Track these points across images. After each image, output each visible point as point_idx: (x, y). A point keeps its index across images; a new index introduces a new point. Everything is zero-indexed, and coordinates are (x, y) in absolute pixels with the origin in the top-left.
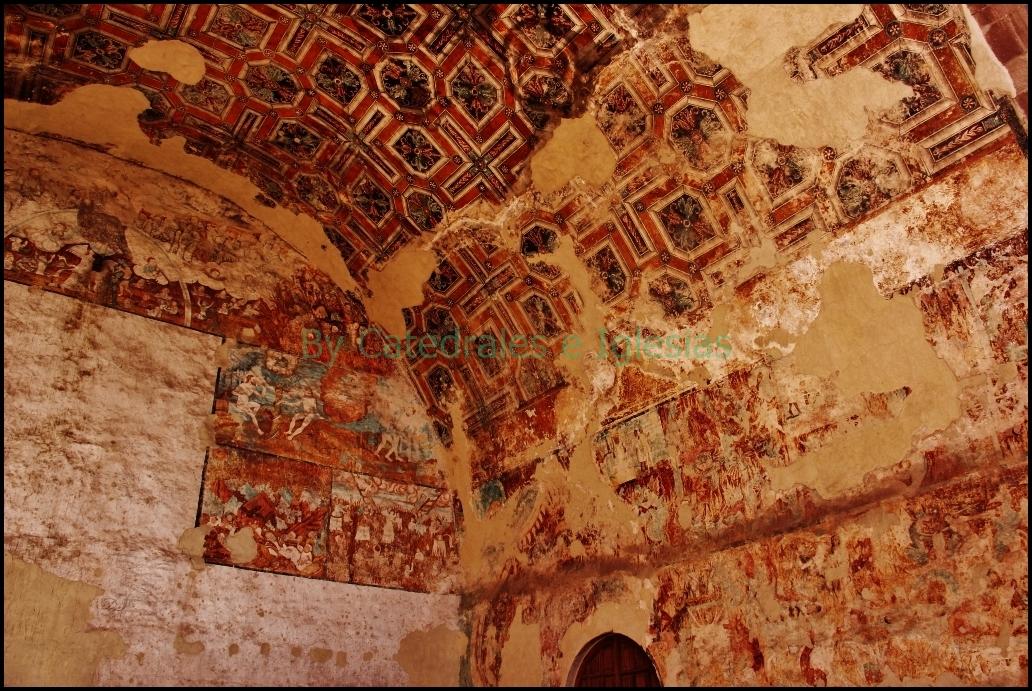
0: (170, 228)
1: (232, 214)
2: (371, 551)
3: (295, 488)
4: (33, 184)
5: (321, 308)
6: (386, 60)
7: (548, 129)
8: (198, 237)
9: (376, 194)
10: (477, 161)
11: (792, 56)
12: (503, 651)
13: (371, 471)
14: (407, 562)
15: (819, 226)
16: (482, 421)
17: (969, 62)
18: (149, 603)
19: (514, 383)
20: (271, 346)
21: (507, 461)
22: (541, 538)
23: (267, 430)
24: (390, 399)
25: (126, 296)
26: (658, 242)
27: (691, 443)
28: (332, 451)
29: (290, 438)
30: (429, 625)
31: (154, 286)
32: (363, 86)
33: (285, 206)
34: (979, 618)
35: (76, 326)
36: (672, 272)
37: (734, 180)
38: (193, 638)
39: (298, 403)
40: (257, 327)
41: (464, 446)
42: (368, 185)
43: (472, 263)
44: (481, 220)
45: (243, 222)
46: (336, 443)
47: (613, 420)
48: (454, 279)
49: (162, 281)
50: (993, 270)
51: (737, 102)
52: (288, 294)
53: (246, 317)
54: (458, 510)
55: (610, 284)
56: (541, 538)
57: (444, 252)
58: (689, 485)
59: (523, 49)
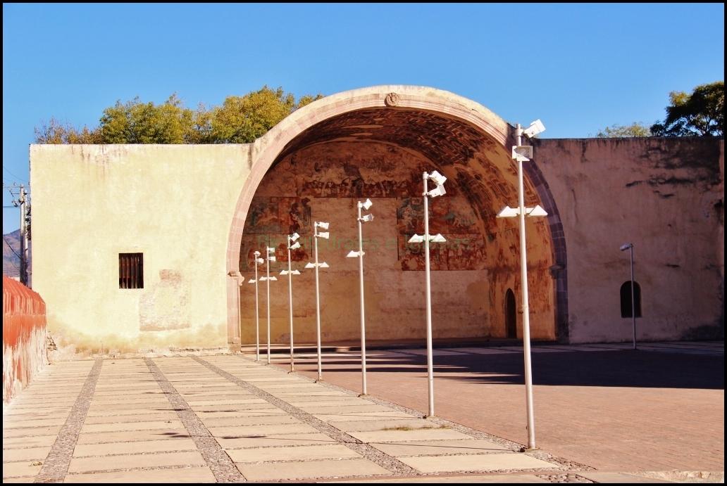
1: (391, 150)
4: (329, 162)
14: (467, 261)
25: (364, 192)
31: (371, 186)
38: (402, 292)
41: (482, 221)
46: (439, 225)
49: (374, 183)
54: (485, 241)
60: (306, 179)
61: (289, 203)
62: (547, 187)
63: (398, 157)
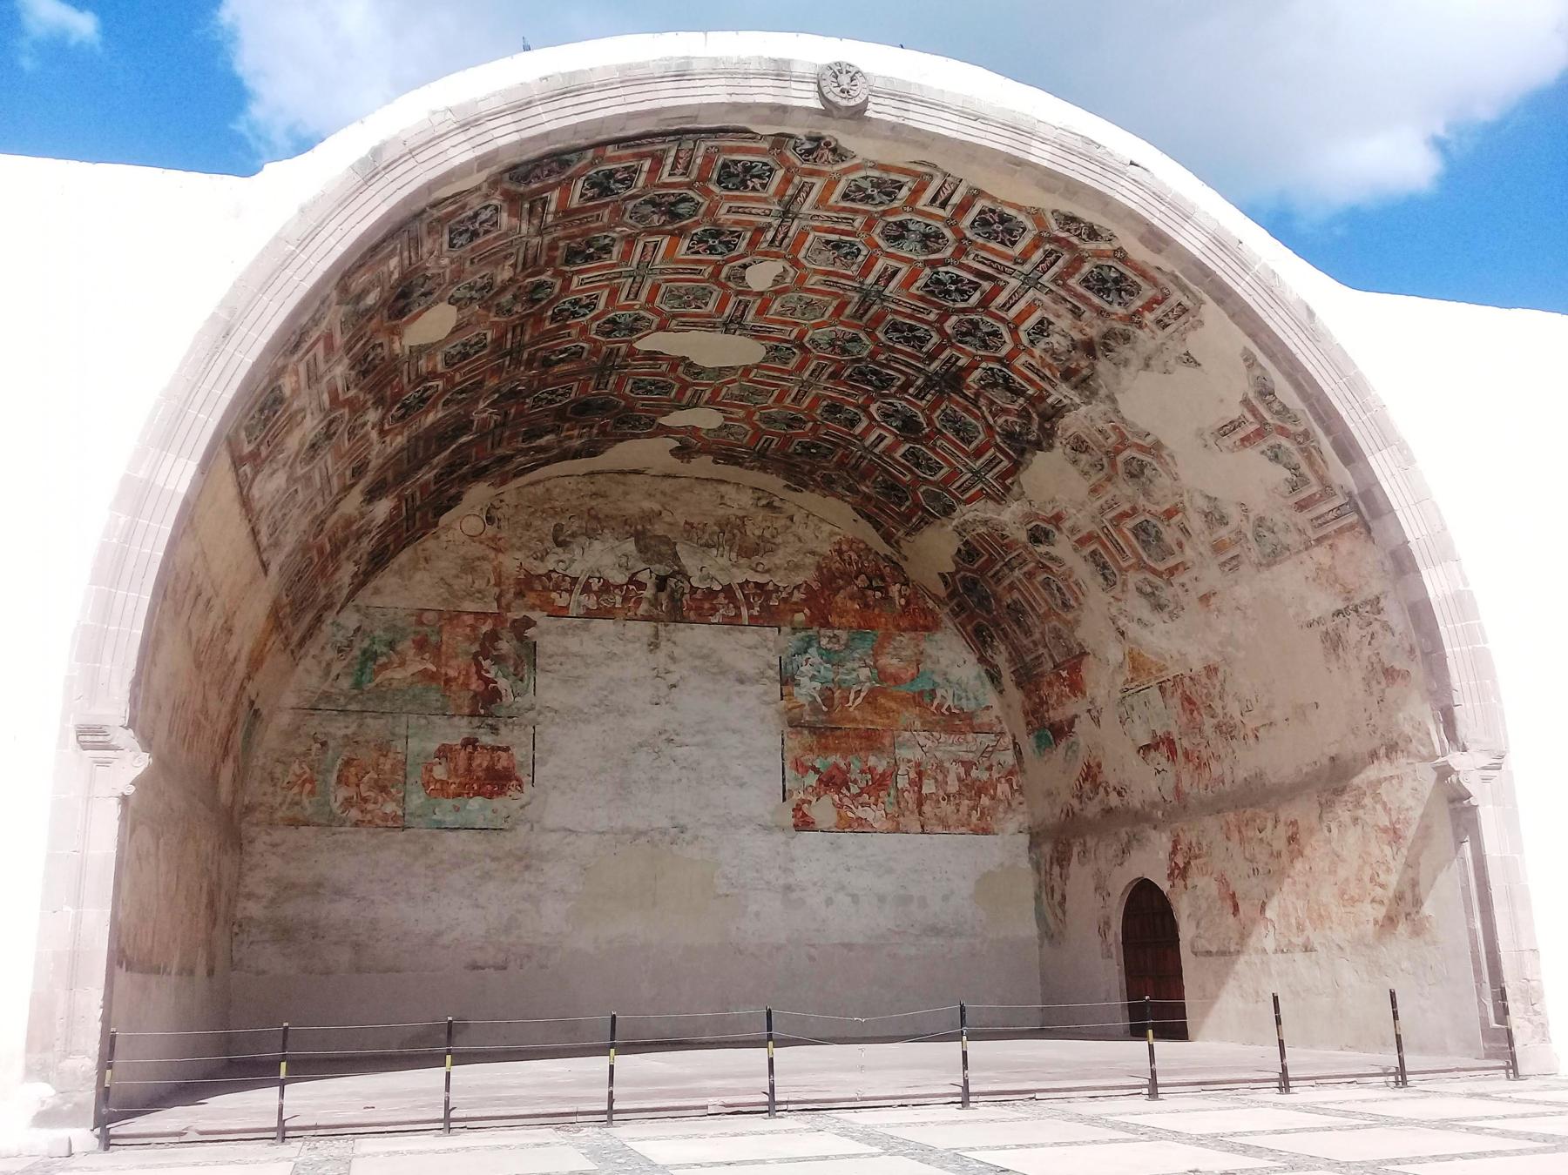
0: (713, 533)
1: (764, 502)
2: (939, 802)
3: (862, 754)
4: (594, 524)
5: (863, 577)
6: (878, 403)
7: (1028, 456)
8: (739, 534)
9: (893, 487)
10: (975, 473)
11: (1200, 434)
12: (1067, 888)
13: (929, 728)
14: (974, 808)
15: (1247, 561)
16: (1026, 674)
17: (1324, 462)
18: (757, 871)
19: (1045, 646)
20: (822, 626)
21: (1051, 713)
22: (1087, 786)
23: (830, 706)
24: (940, 653)
25: (690, 609)
26: (1134, 551)
27: (1184, 719)
28: (891, 714)
29: (851, 709)
30: (1002, 864)
31: (711, 594)
32: (863, 418)
33: (813, 491)
34: (1354, 891)
35: (657, 646)
36: (1150, 577)
37: (1180, 515)
38: (794, 896)
39: (854, 675)
40: (806, 611)
41: (1015, 695)
42: (884, 481)
43: (991, 546)
44: (989, 515)
45: (775, 507)
47: (1128, 690)
48: (978, 555)
50: (1361, 622)
51: (1168, 459)
52: (829, 570)
53: (796, 603)
55: (1106, 579)
56: (1087, 786)
57: (964, 534)
58: (1186, 754)
59: (992, 403)
60: (526, 565)
61: (474, 628)
62: (1410, 460)
63: (781, 522)
